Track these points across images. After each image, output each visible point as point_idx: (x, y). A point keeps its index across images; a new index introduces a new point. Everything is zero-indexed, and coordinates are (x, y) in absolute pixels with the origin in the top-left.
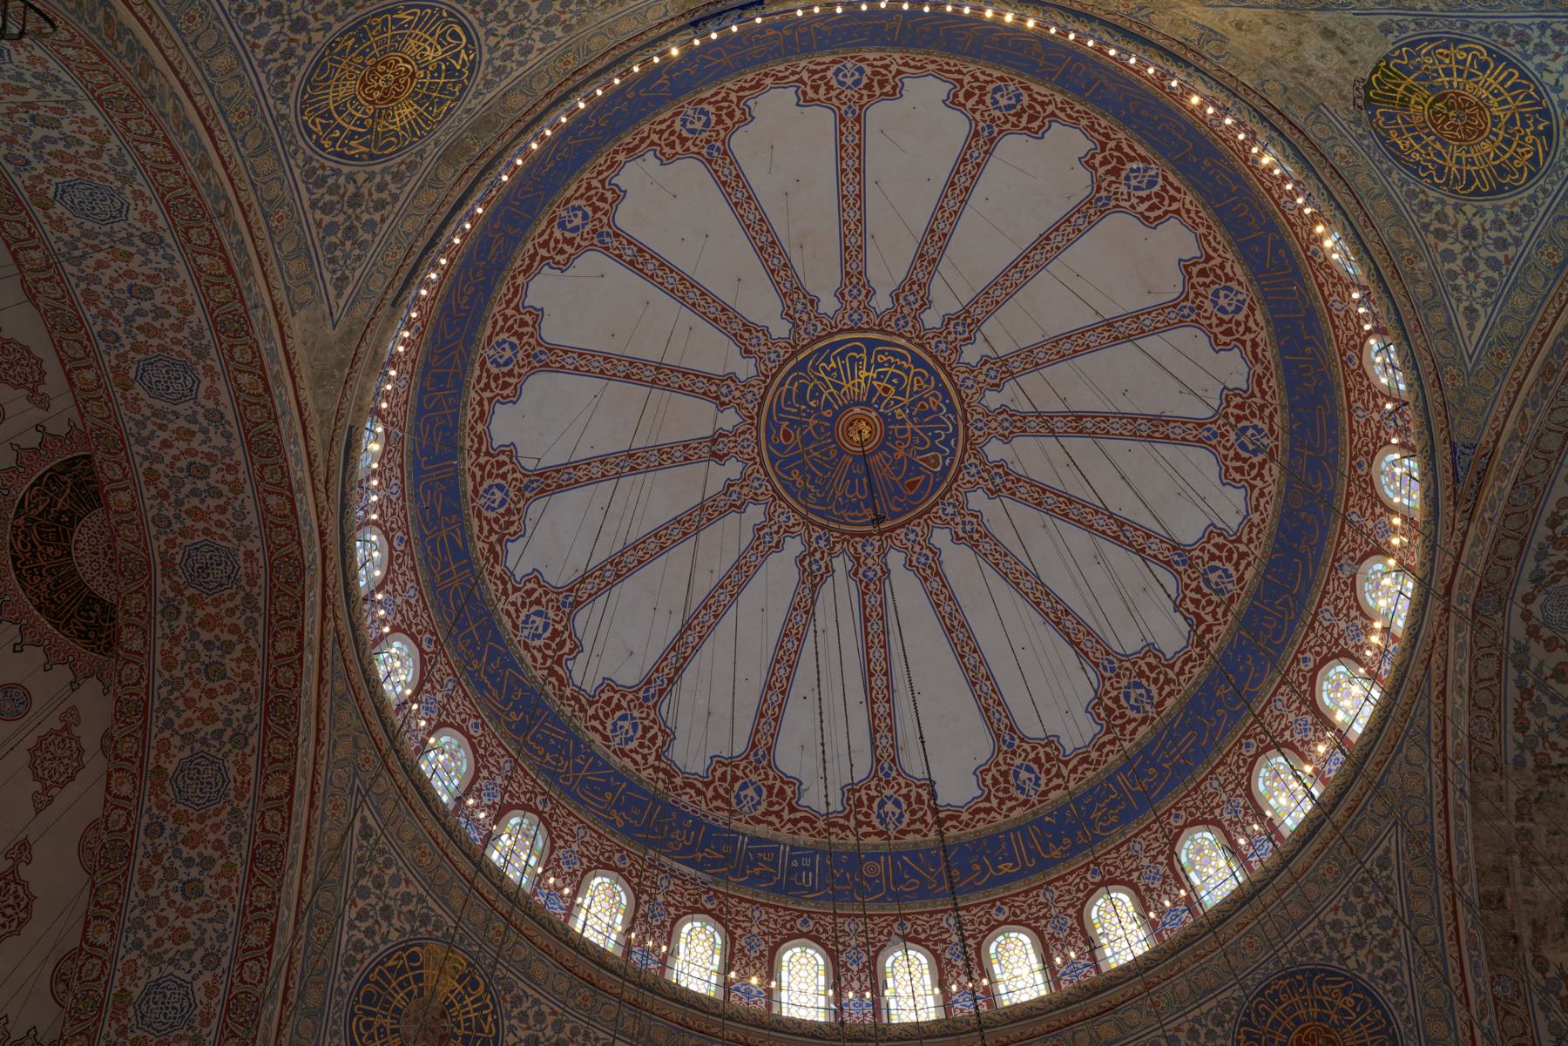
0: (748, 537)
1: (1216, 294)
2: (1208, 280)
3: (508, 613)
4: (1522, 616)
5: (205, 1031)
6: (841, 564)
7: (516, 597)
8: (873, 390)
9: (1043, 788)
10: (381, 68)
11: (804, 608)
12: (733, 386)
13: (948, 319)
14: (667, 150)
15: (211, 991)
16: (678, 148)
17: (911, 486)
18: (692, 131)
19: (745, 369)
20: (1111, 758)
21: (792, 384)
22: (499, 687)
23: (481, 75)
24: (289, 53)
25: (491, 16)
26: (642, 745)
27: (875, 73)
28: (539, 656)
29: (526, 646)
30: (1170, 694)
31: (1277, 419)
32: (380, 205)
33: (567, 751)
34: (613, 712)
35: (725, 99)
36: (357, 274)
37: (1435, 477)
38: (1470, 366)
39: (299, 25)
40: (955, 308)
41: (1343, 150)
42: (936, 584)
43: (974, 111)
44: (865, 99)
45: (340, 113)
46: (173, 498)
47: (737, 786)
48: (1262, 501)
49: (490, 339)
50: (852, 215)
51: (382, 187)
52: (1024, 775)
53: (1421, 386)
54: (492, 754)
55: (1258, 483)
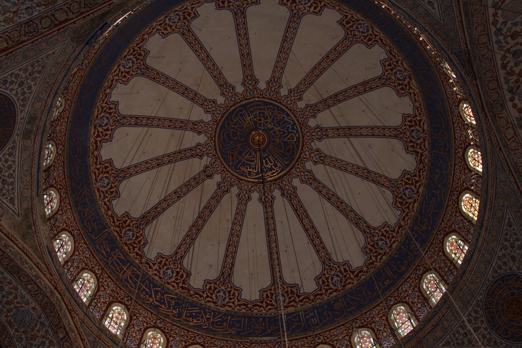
0: (235, 200)
1: (357, 28)
2: (351, 24)
3: (155, 275)
4: (513, 107)
6: (277, 193)
7: (156, 267)
9: (389, 245)
12: (201, 148)
13: (268, 83)
14: (124, 79)
16: (128, 76)
18: (129, 68)
19: (202, 139)
22: (164, 303)
23: (18, 105)
25: (8, 85)
26: (230, 299)
27: (184, 13)
28: (175, 284)
29: (168, 283)
31: (404, 64)
32: (10, 167)
33: (202, 315)
34: (214, 291)
35: (134, 51)
36: (16, 194)
37: (457, 68)
38: (442, 22)
40: (268, 77)
42: (315, 184)
43: (229, 6)
44: (187, 23)
48: (416, 97)
49: (96, 180)
50: (209, 64)
51: (6, 161)
53: (432, 37)
54: (171, 330)
55: (411, 91)
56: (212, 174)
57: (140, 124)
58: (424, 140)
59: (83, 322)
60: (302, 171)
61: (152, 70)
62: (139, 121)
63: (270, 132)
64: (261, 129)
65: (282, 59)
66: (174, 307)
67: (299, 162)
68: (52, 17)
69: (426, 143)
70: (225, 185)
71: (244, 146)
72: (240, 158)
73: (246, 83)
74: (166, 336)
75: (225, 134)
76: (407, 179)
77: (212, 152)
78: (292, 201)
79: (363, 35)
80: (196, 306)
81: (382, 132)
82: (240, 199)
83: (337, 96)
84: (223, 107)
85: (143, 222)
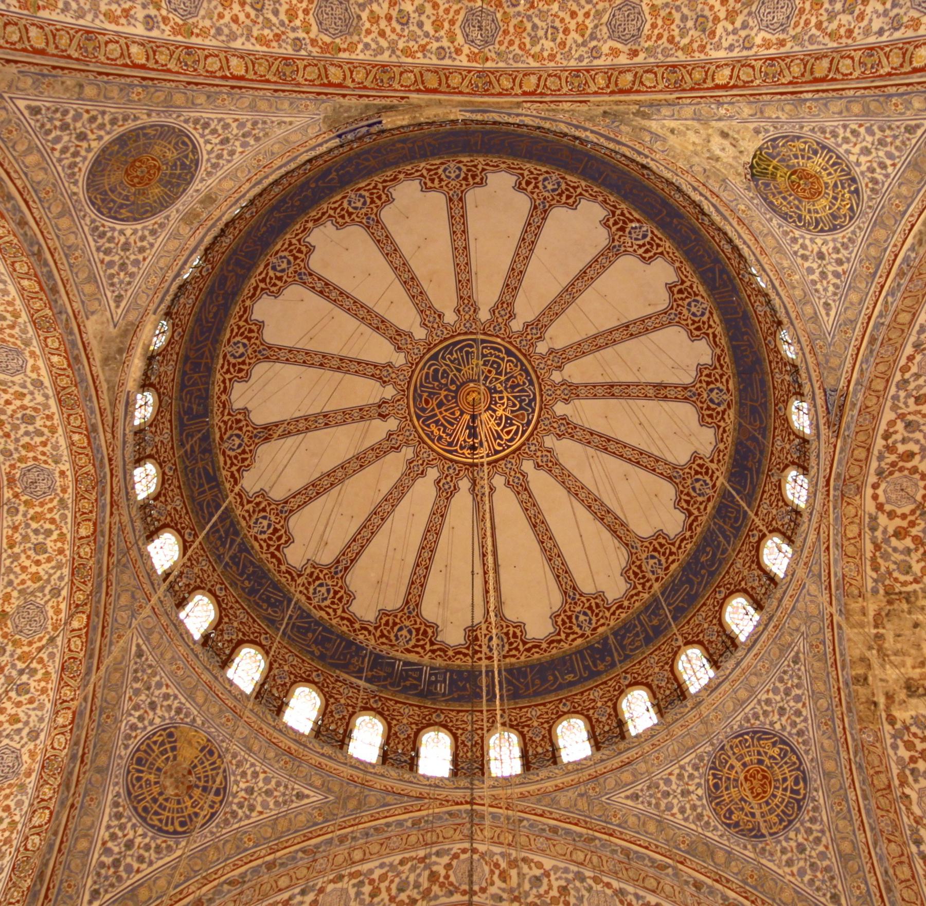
5: (28, 780)
6: (465, 484)
9: (594, 625)
10: (138, 164)
11: (439, 514)
13: (527, 325)
14: (340, 220)
15: (32, 754)
19: (399, 359)
20: (637, 604)
22: (237, 564)
24: (76, 154)
25: (207, 131)
26: (333, 603)
28: (264, 545)
29: (256, 539)
30: (673, 561)
37: (816, 411)
39: (82, 137)
40: (530, 318)
41: (743, 207)
42: (525, 496)
45: (113, 192)
46: (13, 437)
47: (396, 629)
50: (462, 260)
52: (582, 618)
53: (804, 354)
54: (231, 608)
58: (709, 500)
59: (122, 529)
66: (249, 576)
68: (323, 71)
69: (710, 505)
72: (437, 411)
74: (221, 612)
76: (660, 544)
80: (280, 591)
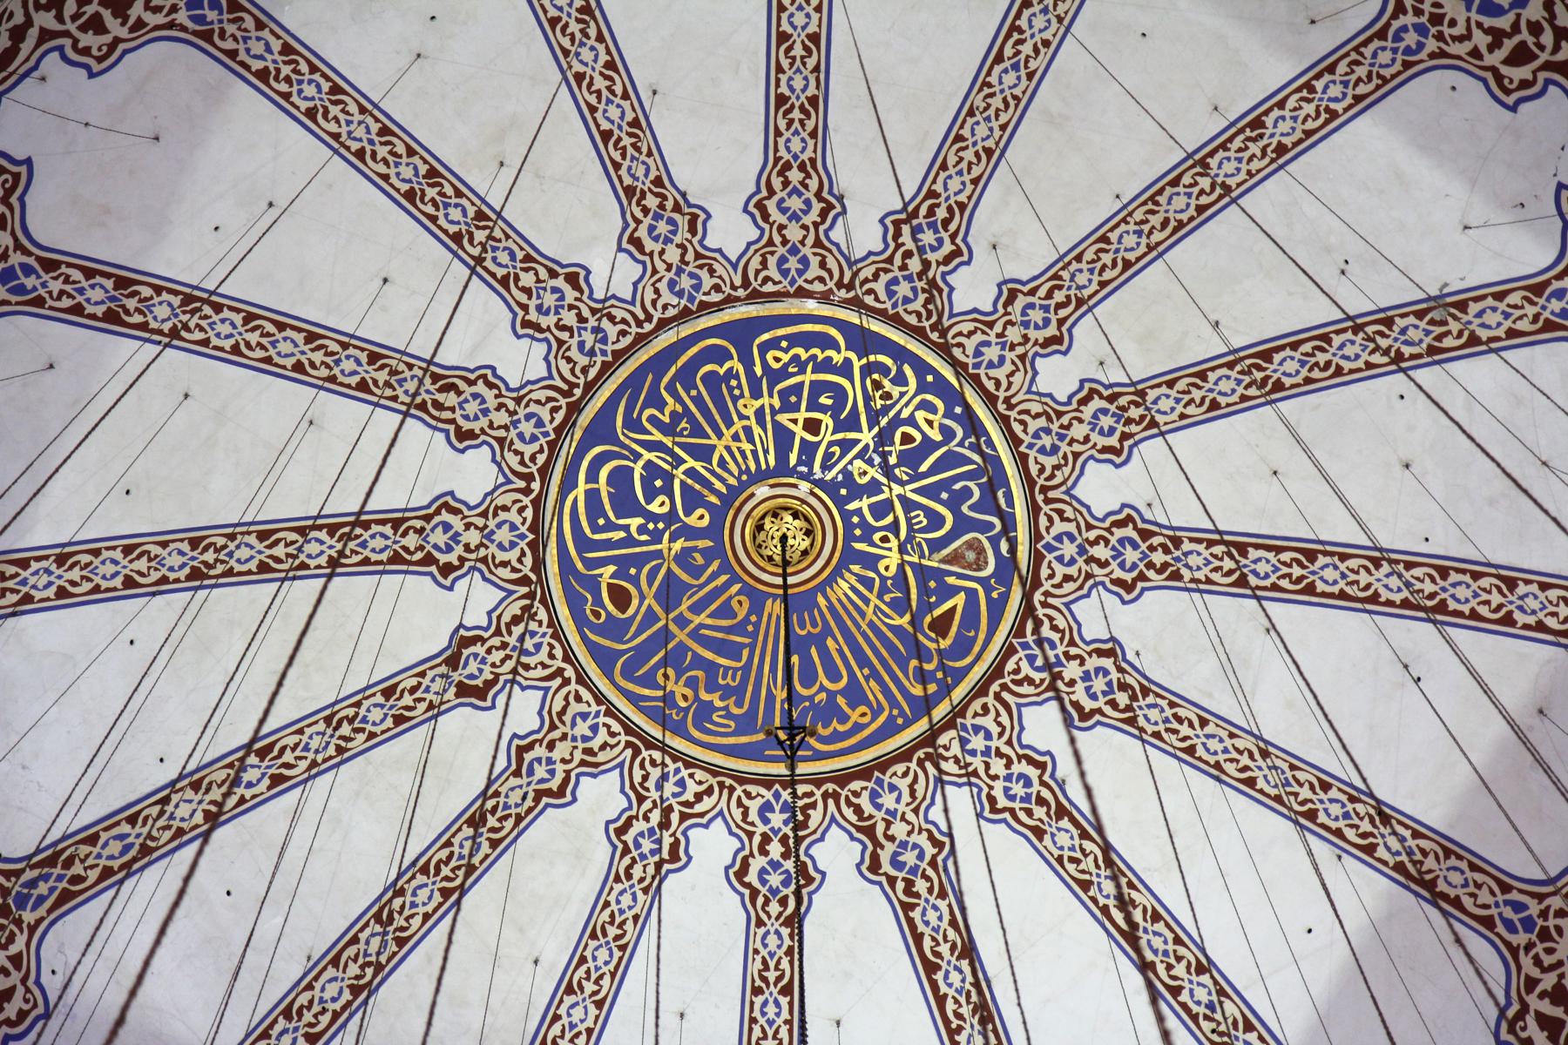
0: (601, 852)
6: (836, 853)
8: (783, 438)
12: (457, 523)
14: (87, 39)
17: (941, 626)
19: (473, 475)
21: (592, 476)
50: (590, 58)
56: (489, 684)
57: (137, 319)
60: (999, 754)
61: (260, 26)
62: (131, 304)
63: (852, 506)
64: (806, 477)
65: (997, 102)
67: (990, 700)
70: (556, 755)
71: (699, 559)
73: (771, 206)
75: (604, 474)
77: (513, 555)
78: (916, 914)
79: (1488, 22)
81: (1496, 599)
82: (626, 851)
83: (1267, 356)
84: (619, 314)
85: (43, 888)
